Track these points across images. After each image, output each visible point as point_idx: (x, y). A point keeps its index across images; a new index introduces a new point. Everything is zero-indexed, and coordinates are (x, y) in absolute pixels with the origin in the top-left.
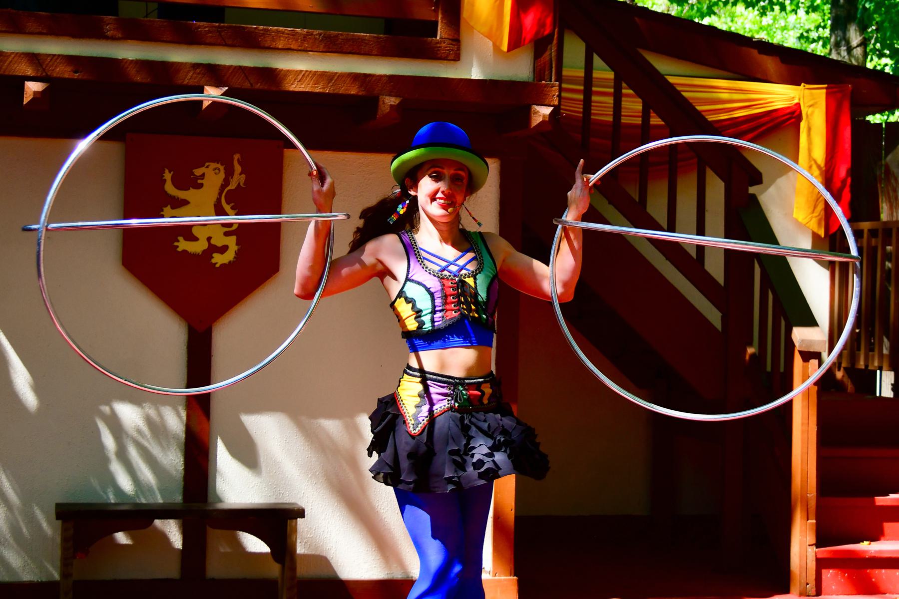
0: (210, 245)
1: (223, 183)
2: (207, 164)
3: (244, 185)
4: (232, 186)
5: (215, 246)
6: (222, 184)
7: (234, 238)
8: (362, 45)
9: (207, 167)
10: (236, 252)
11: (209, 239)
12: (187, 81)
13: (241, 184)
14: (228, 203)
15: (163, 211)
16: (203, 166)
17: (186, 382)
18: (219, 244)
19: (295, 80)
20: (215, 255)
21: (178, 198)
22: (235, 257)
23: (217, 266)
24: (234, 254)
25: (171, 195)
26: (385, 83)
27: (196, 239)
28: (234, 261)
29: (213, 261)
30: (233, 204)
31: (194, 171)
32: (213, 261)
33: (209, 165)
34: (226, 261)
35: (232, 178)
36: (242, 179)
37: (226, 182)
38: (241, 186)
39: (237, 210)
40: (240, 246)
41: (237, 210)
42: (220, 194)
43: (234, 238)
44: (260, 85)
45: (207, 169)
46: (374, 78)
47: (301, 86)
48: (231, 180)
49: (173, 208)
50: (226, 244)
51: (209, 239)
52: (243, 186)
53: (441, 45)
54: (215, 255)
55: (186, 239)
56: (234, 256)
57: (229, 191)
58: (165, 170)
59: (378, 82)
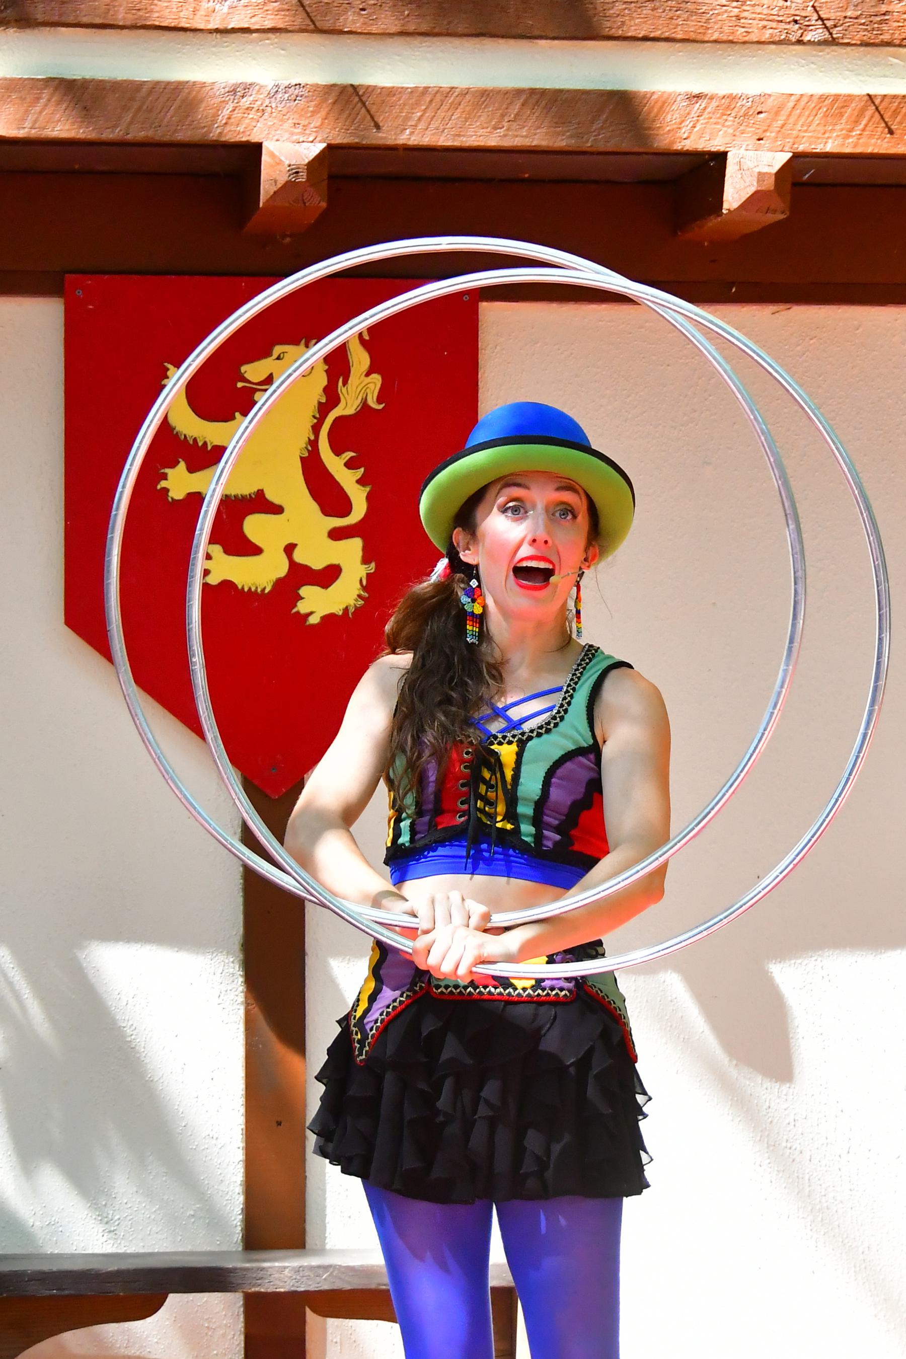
0: (293, 564)
1: (324, 400)
2: (278, 350)
3: (379, 401)
4: (347, 407)
5: (306, 568)
6: (320, 404)
7: (356, 545)
8: (678, 17)
9: (278, 358)
10: (361, 581)
11: (290, 549)
12: (219, 130)
13: (373, 403)
14: (337, 451)
15: (165, 477)
16: (267, 354)
17: (241, 930)
18: (317, 564)
19: (503, 116)
20: (305, 591)
21: (205, 444)
22: (359, 596)
23: (314, 620)
24: (359, 586)
25: (185, 436)
26: (745, 115)
27: (254, 550)
28: (357, 610)
29: (302, 607)
30: (349, 455)
31: (243, 369)
32: (302, 607)
33: (283, 353)
34: (338, 610)
35: (345, 383)
36: (372, 386)
37: (332, 397)
38: (370, 407)
39: (362, 470)
40: (373, 565)
41: (362, 470)
42: (316, 429)
43: (356, 545)
44: (412, 133)
45: (278, 361)
46: (714, 104)
47: (519, 133)
48: (344, 390)
49: (191, 469)
50: (335, 562)
51: (290, 549)
52: (381, 407)
53: (890, 8)
54: (305, 591)
55: (228, 551)
56: (357, 592)
57: (338, 420)
58: (168, 369)
59: (723, 114)
